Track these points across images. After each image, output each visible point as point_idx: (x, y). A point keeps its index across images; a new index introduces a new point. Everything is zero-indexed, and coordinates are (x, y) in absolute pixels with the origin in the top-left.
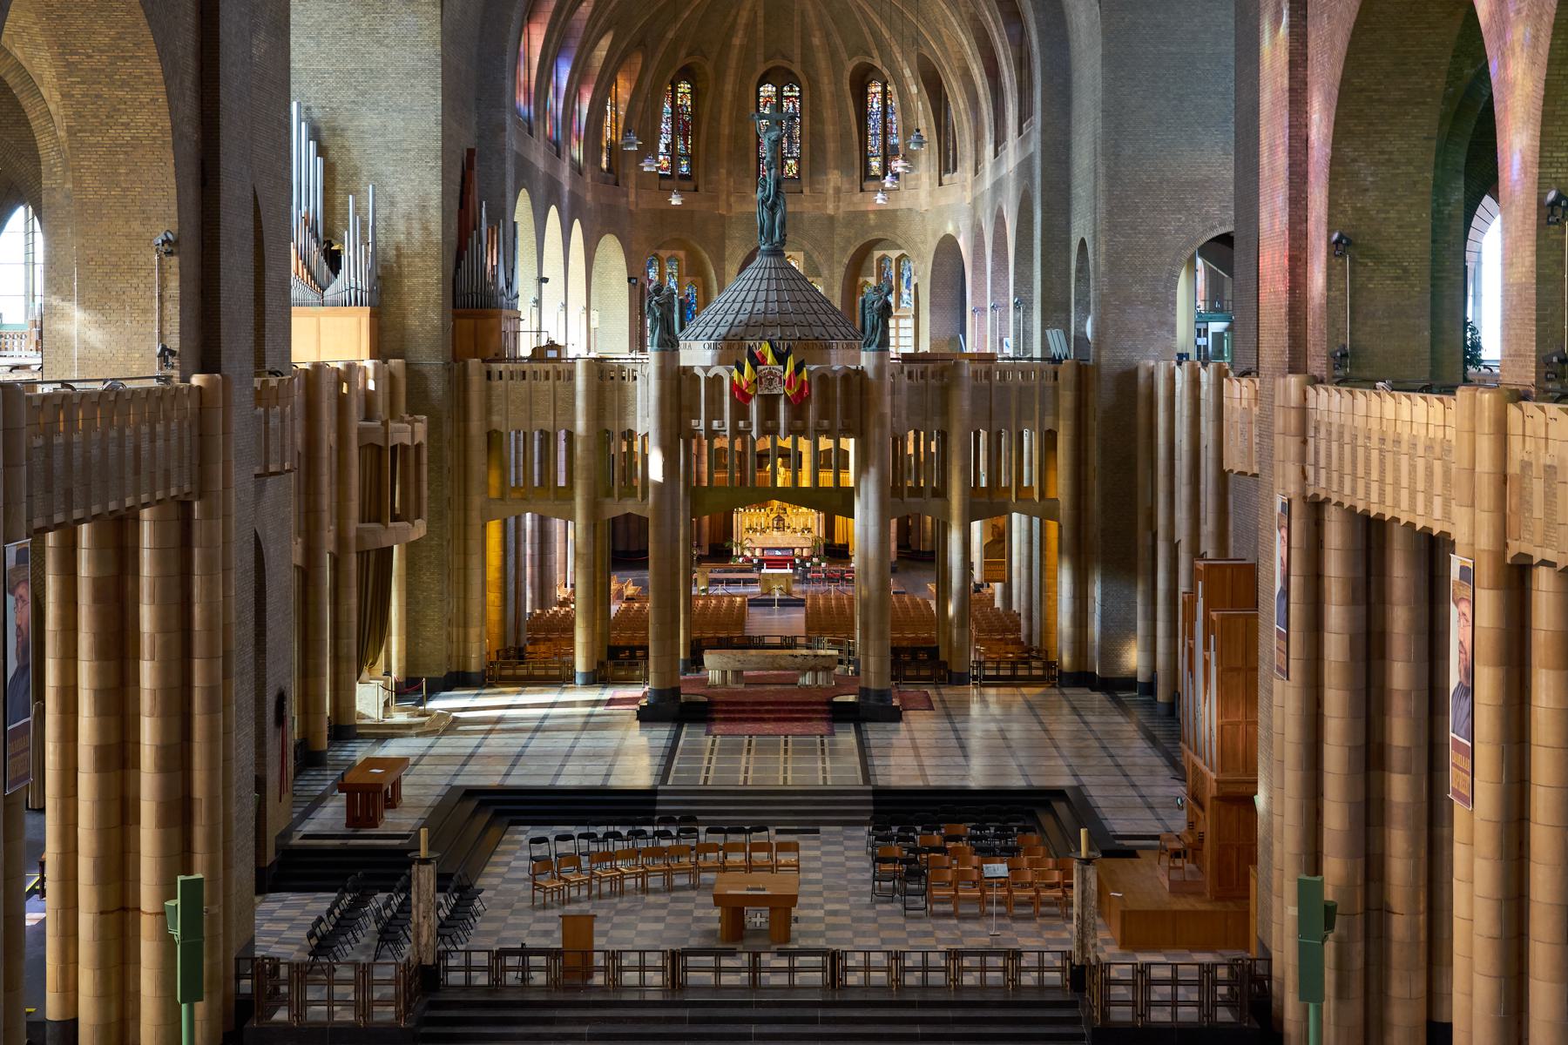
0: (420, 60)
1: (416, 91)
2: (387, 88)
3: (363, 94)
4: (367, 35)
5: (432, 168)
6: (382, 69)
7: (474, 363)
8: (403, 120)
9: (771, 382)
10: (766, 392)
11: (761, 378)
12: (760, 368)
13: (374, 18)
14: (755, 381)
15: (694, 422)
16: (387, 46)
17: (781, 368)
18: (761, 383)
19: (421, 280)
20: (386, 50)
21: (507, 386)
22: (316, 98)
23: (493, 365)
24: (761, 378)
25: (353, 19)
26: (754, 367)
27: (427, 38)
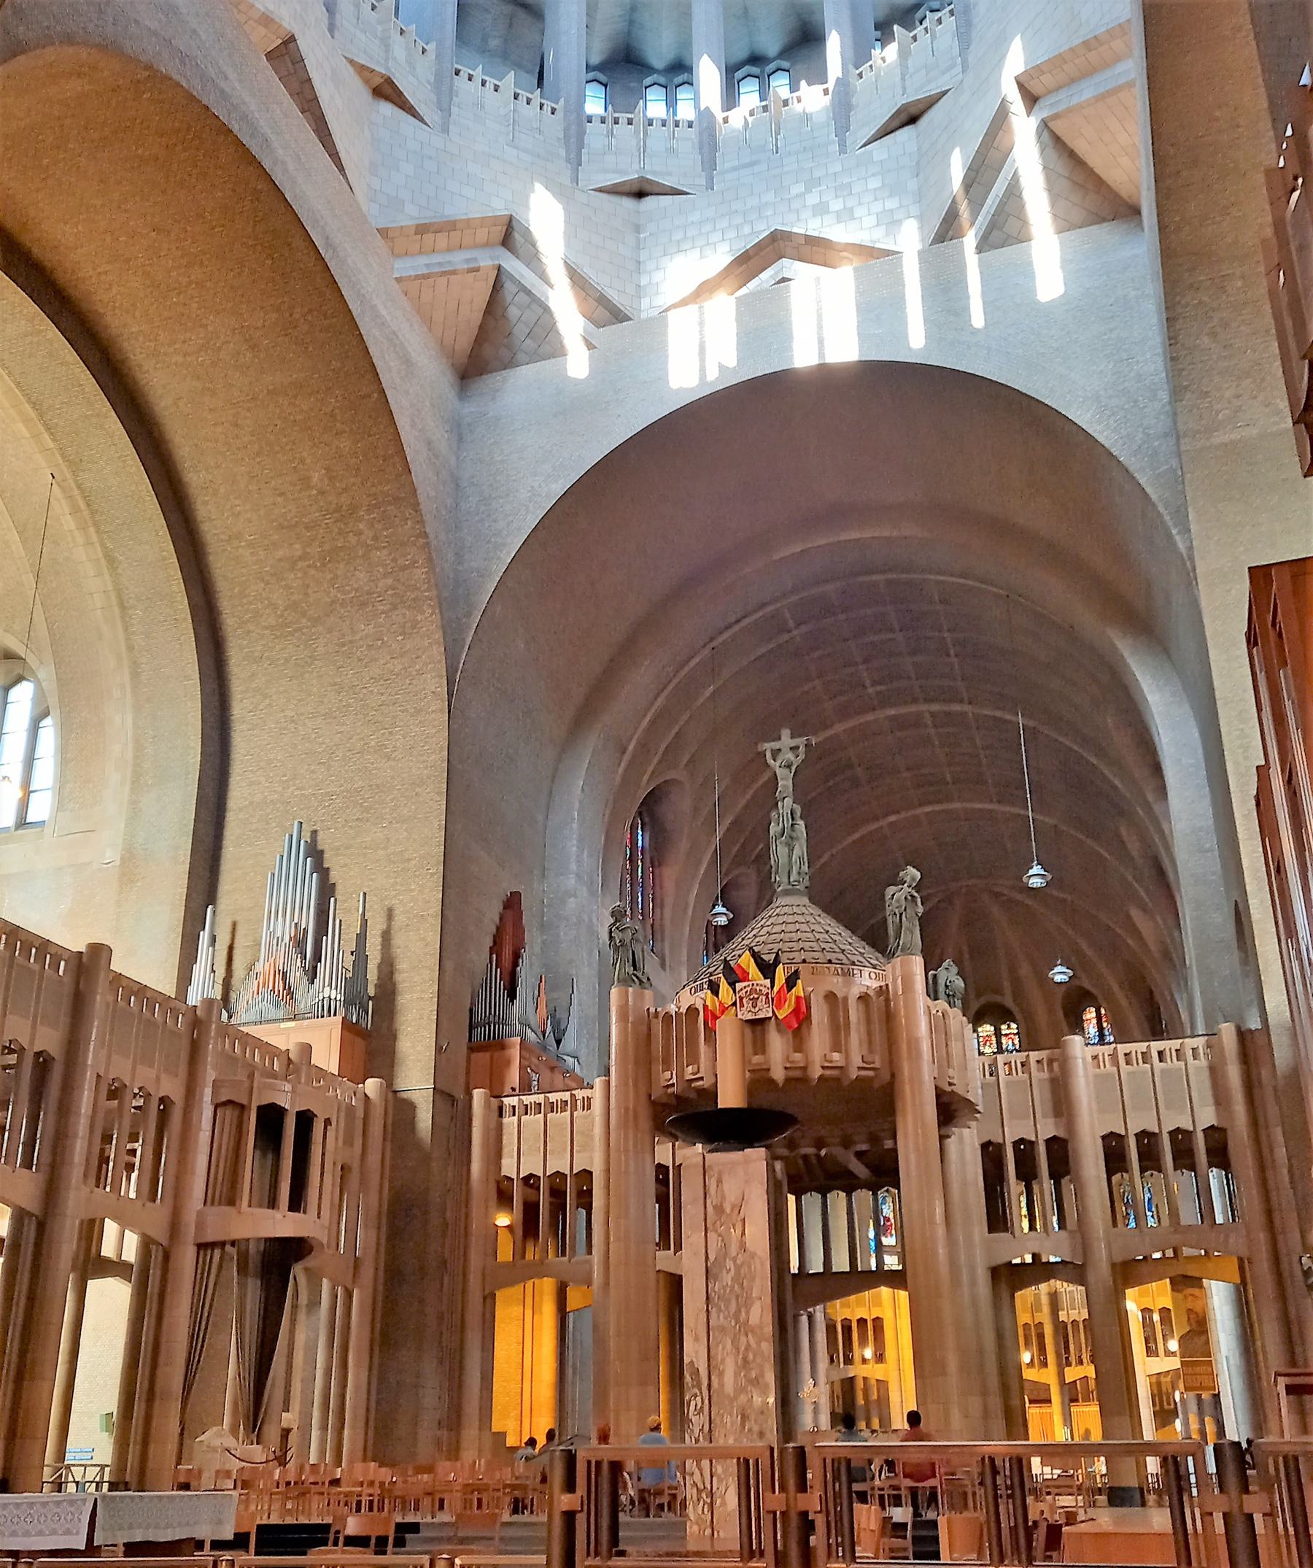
0: (426, 768)
1: (421, 799)
2: (392, 801)
3: (367, 810)
4: (375, 751)
5: (432, 875)
6: (388, 782)
7: (478, 1094)
8: (406, 830)
9: (754, 1001)
10: (750, 1016)
11: (741, 999)
12: (739, 986)
13: (383, 734)
14: (734, 1004)
15: (668, 1074)
16: (394, 760)
17: (768, 982)
18: (742, 1005)
19: (415, 996)
20: (393, 763)
21: (519, 1120)
22: (322, 821)
23: (503, 1099)
24: (741, 999)
25: (362, 739)
26: (732, 985)
27: (434, 746)
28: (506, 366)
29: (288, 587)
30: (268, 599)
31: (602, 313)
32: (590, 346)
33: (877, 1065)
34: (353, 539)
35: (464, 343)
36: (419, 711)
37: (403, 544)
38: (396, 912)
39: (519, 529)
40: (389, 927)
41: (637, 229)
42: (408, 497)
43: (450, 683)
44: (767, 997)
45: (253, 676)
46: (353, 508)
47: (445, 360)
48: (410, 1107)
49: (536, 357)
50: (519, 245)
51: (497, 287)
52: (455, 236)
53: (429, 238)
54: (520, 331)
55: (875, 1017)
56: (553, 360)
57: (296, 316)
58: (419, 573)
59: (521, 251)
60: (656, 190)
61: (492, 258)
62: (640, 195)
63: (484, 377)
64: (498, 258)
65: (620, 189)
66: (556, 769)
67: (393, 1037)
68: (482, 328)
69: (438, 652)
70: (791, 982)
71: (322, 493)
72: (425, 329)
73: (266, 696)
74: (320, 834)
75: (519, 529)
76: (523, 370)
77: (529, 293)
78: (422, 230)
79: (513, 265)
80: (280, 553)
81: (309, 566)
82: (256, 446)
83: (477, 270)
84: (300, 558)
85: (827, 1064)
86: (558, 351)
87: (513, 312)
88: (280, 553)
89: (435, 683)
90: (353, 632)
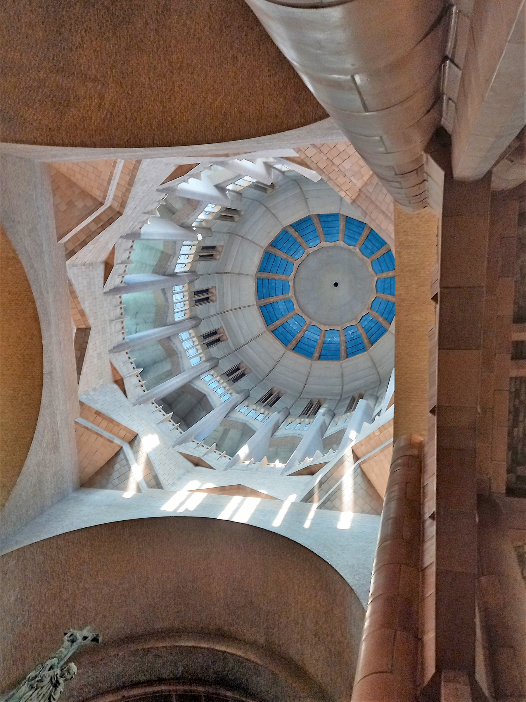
31: (153, 482)
35: (91, 470)
49: (116, 487)
51: (117, 454)
54: (115, 475)
57: (19, 395)
63: (91, 490)
72: (76, 451)
83: (112, 442)
87: (117, 466)
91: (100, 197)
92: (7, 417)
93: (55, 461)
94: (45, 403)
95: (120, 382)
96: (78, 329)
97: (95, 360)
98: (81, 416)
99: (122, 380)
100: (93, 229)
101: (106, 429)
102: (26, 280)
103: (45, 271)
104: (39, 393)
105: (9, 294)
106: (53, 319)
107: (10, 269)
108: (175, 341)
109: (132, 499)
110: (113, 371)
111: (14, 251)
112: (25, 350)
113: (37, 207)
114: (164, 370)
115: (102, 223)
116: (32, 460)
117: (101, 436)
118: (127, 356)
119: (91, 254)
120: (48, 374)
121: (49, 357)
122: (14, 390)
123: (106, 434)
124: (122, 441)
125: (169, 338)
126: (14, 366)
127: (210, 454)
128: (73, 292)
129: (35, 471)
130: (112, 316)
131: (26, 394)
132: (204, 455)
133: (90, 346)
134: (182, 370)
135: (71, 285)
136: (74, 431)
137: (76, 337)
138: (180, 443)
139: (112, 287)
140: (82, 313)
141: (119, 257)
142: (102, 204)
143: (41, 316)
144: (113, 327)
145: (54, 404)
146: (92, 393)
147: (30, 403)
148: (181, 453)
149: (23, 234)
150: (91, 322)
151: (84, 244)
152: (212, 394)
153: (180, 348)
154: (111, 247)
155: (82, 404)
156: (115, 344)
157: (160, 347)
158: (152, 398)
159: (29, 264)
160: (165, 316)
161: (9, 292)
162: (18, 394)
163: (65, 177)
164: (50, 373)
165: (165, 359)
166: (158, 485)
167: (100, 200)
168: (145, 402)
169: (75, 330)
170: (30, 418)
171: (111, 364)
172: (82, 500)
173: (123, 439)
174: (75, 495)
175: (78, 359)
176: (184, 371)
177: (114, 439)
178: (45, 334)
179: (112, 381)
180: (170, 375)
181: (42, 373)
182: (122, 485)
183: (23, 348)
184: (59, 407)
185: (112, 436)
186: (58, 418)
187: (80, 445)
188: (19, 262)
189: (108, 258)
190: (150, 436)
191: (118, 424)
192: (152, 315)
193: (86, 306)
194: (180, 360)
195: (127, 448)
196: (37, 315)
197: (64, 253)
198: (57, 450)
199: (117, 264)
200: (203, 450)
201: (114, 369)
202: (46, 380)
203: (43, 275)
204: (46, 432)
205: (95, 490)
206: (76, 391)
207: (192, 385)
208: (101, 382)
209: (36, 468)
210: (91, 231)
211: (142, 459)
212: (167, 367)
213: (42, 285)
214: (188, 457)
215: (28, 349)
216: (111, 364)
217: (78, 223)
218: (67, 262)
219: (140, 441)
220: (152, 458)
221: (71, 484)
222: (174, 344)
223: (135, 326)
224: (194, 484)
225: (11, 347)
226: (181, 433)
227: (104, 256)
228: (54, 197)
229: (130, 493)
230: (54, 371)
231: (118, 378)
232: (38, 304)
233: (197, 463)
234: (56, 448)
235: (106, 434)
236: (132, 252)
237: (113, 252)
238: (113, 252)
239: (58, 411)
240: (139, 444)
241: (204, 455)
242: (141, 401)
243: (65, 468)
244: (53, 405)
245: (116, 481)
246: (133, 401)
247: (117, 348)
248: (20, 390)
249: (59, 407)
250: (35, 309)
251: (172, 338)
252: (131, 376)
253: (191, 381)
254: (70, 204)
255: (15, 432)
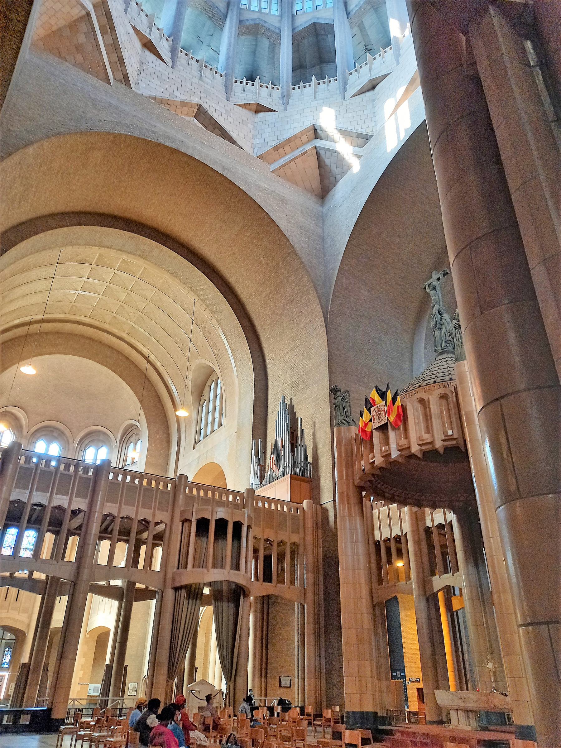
10: (378, 425)
12: (372, 409)
14: (371, 420)
18: (374, 420)
20: (311, 360)
26: (369, 410)
28: (335, 185)
29: (270, 306)
30: (266, 314)
31: (361, 141)
32: (359, 157)
33: (455, 436)
34: (282, 277)
35: (316, 184)
36: (317, 335)
37: (297, 270)
38: (317, 423)
39: (343, 244)
40: (314, 431)
41: (374, 100)
42: (292, 250)
43: (326, 319)
44: (385, 411)
45: (269, 345)
46: (278, 264)
47: (309, 194)
48: (325, 511)
49: (343, 173)
50: (321, 134)
51: (318, 155)
52: (292, 144)
53: (281, 150)
54: (333, 167)
55: (452, 406)
56: (349, 171)
57: (228, 202)
58: (305, 279)
59: (323, 136)
60: (378, 81)
61: (311, 145)
62: (373, 88)
63: (331, 193)
64: (314, 144)
65: (363, 90)
66: (412, 344)
67: (319, 479)
68: (320, 174)
69: (318, 308)
70: (394, 400)
71: (267, 264)
72: (294, 186)
73: (274, 351)
74: (293, 399)
75: (343, 244)
76: (340, 182)
77: (329, 150)
78: (276, 148)
79: (319, 143)
80: (264, 295)
81: (273, 295)
82: (243, 258)
83: (306, 152)
84: (270, 293)
85: (421, 443)
86: (349, 168)
87: (327, 161)
88: (264, 295)
89: (320, 322)
90: (293, 314)
91: (80, 11)
92: (239, 220)
93: (293, 207)
94: (246, 188)
95: (259, 109)
96: (195, 117)
97: (230, 119)
98: (270, 164)
99: (258, 104)
100: (111, 41)
101: (292, 151)
102: (138, 139)
103: (135, 116)
104: (231, 183)
105: (143, 159)
106: (180, 136)
107: (122, 146)
108: (247, 16)
109: (362, 167)
110: (246, 108)
111: (109, 134)
112: (195, 176)
113: (73, 85)
114: (267, 49)
115: (108, 26)
116: (282, 223)
117: (296, 158)
118: (238, 83)
119: (132, 58)
120: (224, 171)
121: (210, 161)
122: (222, 203)
123: (297, 153)
124: (310, 143)
125: (241, 22)
126: (203, 192)
127: (373, 66)
128: (162, 101)
129: (291, 227)
130: (197, 74)
131: (231, 197)
132: (371, 74)
133: (215, 116)
134: (277, 31)
135: (154, 99)
136: (278, 177)
137: (202, 123)
138: (345, 90)
139: (170, 54)
140: (184, 104)
141: (144, 30)
142: (88, 14)
143: (174, 146)
144: (207, 80)
145: (249, 181)
146: (256, 142)
147: (239, 199)
148: (354, 96)
149: (96, 115)
150: (194, 100)
151: (121, 60)
152: (318, 15)
153: (255, 16)
154: (132, 31)
155: (260, 157)
156: (222, 89)
157: (243, 38)
158: (288, 87)
159: (125, 128)
160: (216, 9)
161: (142, 158)
162: (226, 202)
163: (49, 35)
164: (224, 168)
165: (256, 40)
166: (367, 138)
167: (84, 13)
168: (288, 96)
169: (196, 121)
170: (251, 206)
171: (239, 105)
172: (334, 206)
173: (309, 141)
174: (326, 208)
175: (222, 136)
176: (280, 29)
177: (304, 149)
178: (190, 152)
179: (254, 114)
180: (274, 46)
181: (222, 175)
182: (345, 167)
183: (193, 176)
184: (254, 178)
185: (301, 149)
186: (263, 185)
187: (292, 180)
188: (120, 135)
189: (141, 40)
190: (321, 114)
191: (295, 137)
192: (209, 23)
193: (179, 96)
194: (266, 25)
195: (319, 143)
196: (171, 148)
197: (123, 85)
198: (286, 200)
199: (150, 34)
200: (365, 69)
201: (244, 106)
202: (228, 176)
203: (138, 121)
204: (268, 201)
205: (333, 190)
206: (249, 155)
207: (297, 30)
208: (250, 126)
209: (290, 225)
210: (111, 44)
211: (336, 136)
212: (265, 43)
213: (147, 128)
214: (361, 92)
215: (195, 173)
216: (239, 105)
217: (101, 54)
218: (133, 89)
219: (321, 126)
220: (342, 126)
221: (316, 205)
222: (247, 20)
223: (210, 48)
224: (389, 105)
225: (186, 184)
226: (336, 80)
227: (138, 44)
228: (66, 61)
229: (356, 166)
230: (224, 164)
231: (254, 107)
232: (162, 142)
233: (372, 86)
234: (283, 201)
235: (297, 153)
236: (143, 7)
237: (137, 32)
238: (137, 32)
239: (257, 181)
240: (323, 131)
241: (371, 74)
242: (286, 100)
243: (302, 203)
244: (250, 182)
245: (339, 170)
246: (282, 107)
247: (228, 90)
248: (225, 200)
249: (254, 178)
250: (166, 147)
251: (241, 19)
252: (259, 94)
253: (293, 29)
254: (79, 48)
255: (255, 223)
